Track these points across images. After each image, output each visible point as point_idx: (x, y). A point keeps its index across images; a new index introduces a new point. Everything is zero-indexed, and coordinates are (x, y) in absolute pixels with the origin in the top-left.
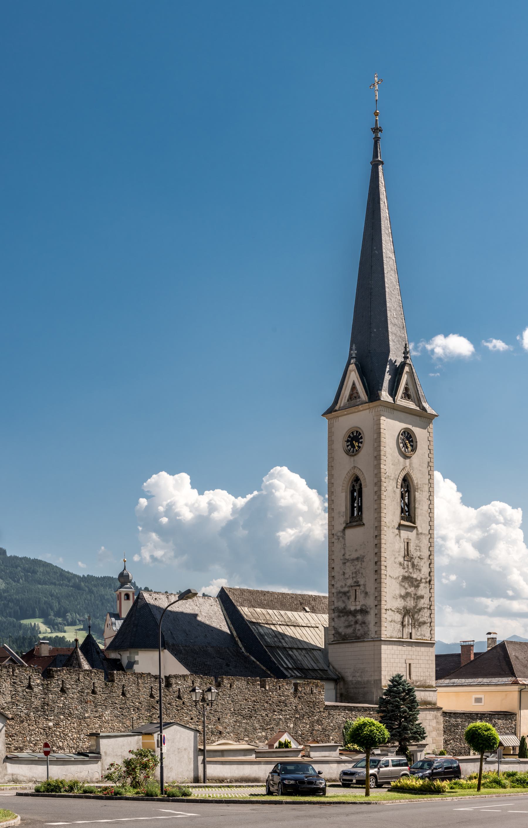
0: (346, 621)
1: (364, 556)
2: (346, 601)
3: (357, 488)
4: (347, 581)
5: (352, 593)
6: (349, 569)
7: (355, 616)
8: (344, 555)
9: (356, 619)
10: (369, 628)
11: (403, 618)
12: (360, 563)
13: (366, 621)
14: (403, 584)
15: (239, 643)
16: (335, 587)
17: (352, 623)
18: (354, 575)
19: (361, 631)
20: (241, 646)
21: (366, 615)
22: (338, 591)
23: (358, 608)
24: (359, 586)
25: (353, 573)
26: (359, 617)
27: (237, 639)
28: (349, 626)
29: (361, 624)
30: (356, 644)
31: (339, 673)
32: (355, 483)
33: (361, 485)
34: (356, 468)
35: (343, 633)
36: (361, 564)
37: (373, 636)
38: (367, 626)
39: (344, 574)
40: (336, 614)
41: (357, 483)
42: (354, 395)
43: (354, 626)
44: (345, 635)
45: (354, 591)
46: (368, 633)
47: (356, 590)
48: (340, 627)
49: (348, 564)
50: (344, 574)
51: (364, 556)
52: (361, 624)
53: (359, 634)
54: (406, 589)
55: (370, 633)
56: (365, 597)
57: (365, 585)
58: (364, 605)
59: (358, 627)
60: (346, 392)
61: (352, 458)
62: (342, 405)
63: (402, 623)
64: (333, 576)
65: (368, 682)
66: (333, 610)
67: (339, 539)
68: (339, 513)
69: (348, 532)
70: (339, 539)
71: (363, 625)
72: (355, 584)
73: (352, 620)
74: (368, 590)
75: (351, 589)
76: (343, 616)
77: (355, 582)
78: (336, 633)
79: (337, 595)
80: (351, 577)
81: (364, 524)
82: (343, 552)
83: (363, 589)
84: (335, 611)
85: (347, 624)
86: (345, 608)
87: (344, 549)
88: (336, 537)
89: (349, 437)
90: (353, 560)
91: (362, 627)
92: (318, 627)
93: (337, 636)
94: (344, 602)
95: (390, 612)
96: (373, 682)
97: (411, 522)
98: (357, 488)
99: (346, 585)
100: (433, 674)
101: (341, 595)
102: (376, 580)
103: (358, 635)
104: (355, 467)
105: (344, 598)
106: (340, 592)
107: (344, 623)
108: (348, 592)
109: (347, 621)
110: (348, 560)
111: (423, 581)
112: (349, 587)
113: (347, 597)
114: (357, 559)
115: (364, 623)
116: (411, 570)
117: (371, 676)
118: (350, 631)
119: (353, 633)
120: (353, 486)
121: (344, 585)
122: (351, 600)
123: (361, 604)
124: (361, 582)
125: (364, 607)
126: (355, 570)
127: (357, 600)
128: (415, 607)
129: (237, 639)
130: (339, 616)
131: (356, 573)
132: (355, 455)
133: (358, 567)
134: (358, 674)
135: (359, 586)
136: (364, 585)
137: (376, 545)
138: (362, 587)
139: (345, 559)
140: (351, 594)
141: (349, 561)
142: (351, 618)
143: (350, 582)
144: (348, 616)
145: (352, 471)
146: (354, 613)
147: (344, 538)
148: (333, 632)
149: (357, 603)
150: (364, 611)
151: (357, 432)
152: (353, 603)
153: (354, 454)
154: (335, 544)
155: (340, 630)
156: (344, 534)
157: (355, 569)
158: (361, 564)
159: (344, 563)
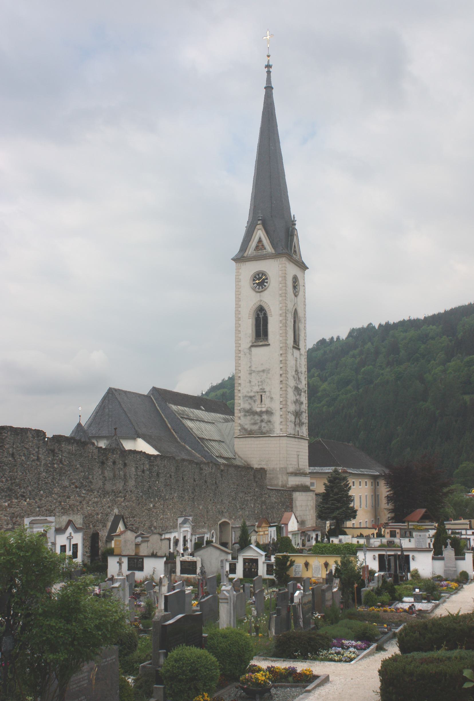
0: (252, 419)
1: (269, 370)
2: (253, 403)
4: (254, 387)
5: (258, 398)
7: (261, 416)
8: (250, 367)
9: (262, 418)
10: (274, 426)
11: (295, 419)
12: (265, 374)
13: (272, 420)
14: (295, 392)
15: (174, 433)
16: (241, 392)
17: (259, 421)
18: (260, 384)
19: (267, 428)
20: (176, 436)
21: (271, 415)
22: (245, 395)
23: (264, 409)
24: (265, 392)
25: (258, 382)
26: (265, 417)
27: (172, 431)
28: (255, 424)
29: (266, 423)
30: (262, 438)
31: (245, 461)
32: (258, 312)
33: (265, 314)
34: (262, 302)
35: (249, 429)
36: (267, 375)
37: (278, 432)
38: (272, 424)
39: (250, 382)
41: (261, 313)
42: (260, 245)
43: (259, 424)
44: (251, 431)
45: (260, 396)
46: (274, 430)
47: (261, 396)
48: (246, 424)
49: (253, 374)
50: (250, 382)
51: (269, 370)
52: (266, 423)
53: (264, 430)
54: (296, 396)
55: (275, 430)
56: (271, 401)
57: (270, 392)
58: (270, 407)
59: (263, 424)
61: (258, 294)
62: (250, 253)
63: (295, 422)
64: (240, 384)
65: (274, 469)
66: (240, 410)
67: (245, 354)
69: (253, 349)
70: (245, 354)
71: (269, 423)
72: (261, 391)
73: (258, 419)
74: (273, 396)
75: (256, 394)
76: (249, 415)
77: (261, 389)
78: (242, 429)
79: (244, 399)
80: (257, 385)
81: (269, 345)
82: (249, 365)
83: (269, 395)
84: (241, 411)
85: (253, 422)
86: (251, 409)
87: (251, 362)
88: (242, 353)
91: (268, 425)
92: (214, 423)
93: (243, 431)
94: (250, 404)
95: (289, 414)
96: (278, 470)
97: (296, 345)
99: (251, 391)
100: (307, 464)
101: (247, 398)
102: (281, 388)
103: (264, 431)
104: (261, 301)
105: (250, 401)
106: (246, 396)
107: (250, 421)
108: (254, 396)
109: (254, 419)
110: (254, 371)
111: (303, 390)
113: (253, 401)
114: (263, 371)
115: (270, 421)
116: (298, 382)
117: (277, 464)
118: (255, 428)
119: (259, 429)
120: (258, 315)
121: (250, 391)
122: (257, 403)
123: (266, 407)
124: (267, 389)
125: (269, 409)
126: (261, 380)
127: (263, 403)
128: (300, 410)
129: (172, 431)
130: (245, 415)
131: (262, 382)
132: (262, 292)
134: (264, 463)
135: (265, 392)
136: (269, 391)
137: (281, 361)
138: (267, 393)
139: (252, 370)
140: (257, 398)
141: (255, 372)
142: (257, 417)
143: (256, 389)
144: (254, 415)
145: (259, 303)
146: (260, 414)
147: (250, 354)
148: (239, 428)
149: (263, 406)
150: (269, 412)
152: (260, 406)
153: (260, 290)
154: (241, 359)
155: (246, 427)
156: (251, 351)
157: (261, 378)
158: (267, 375)
159: (250, 374)
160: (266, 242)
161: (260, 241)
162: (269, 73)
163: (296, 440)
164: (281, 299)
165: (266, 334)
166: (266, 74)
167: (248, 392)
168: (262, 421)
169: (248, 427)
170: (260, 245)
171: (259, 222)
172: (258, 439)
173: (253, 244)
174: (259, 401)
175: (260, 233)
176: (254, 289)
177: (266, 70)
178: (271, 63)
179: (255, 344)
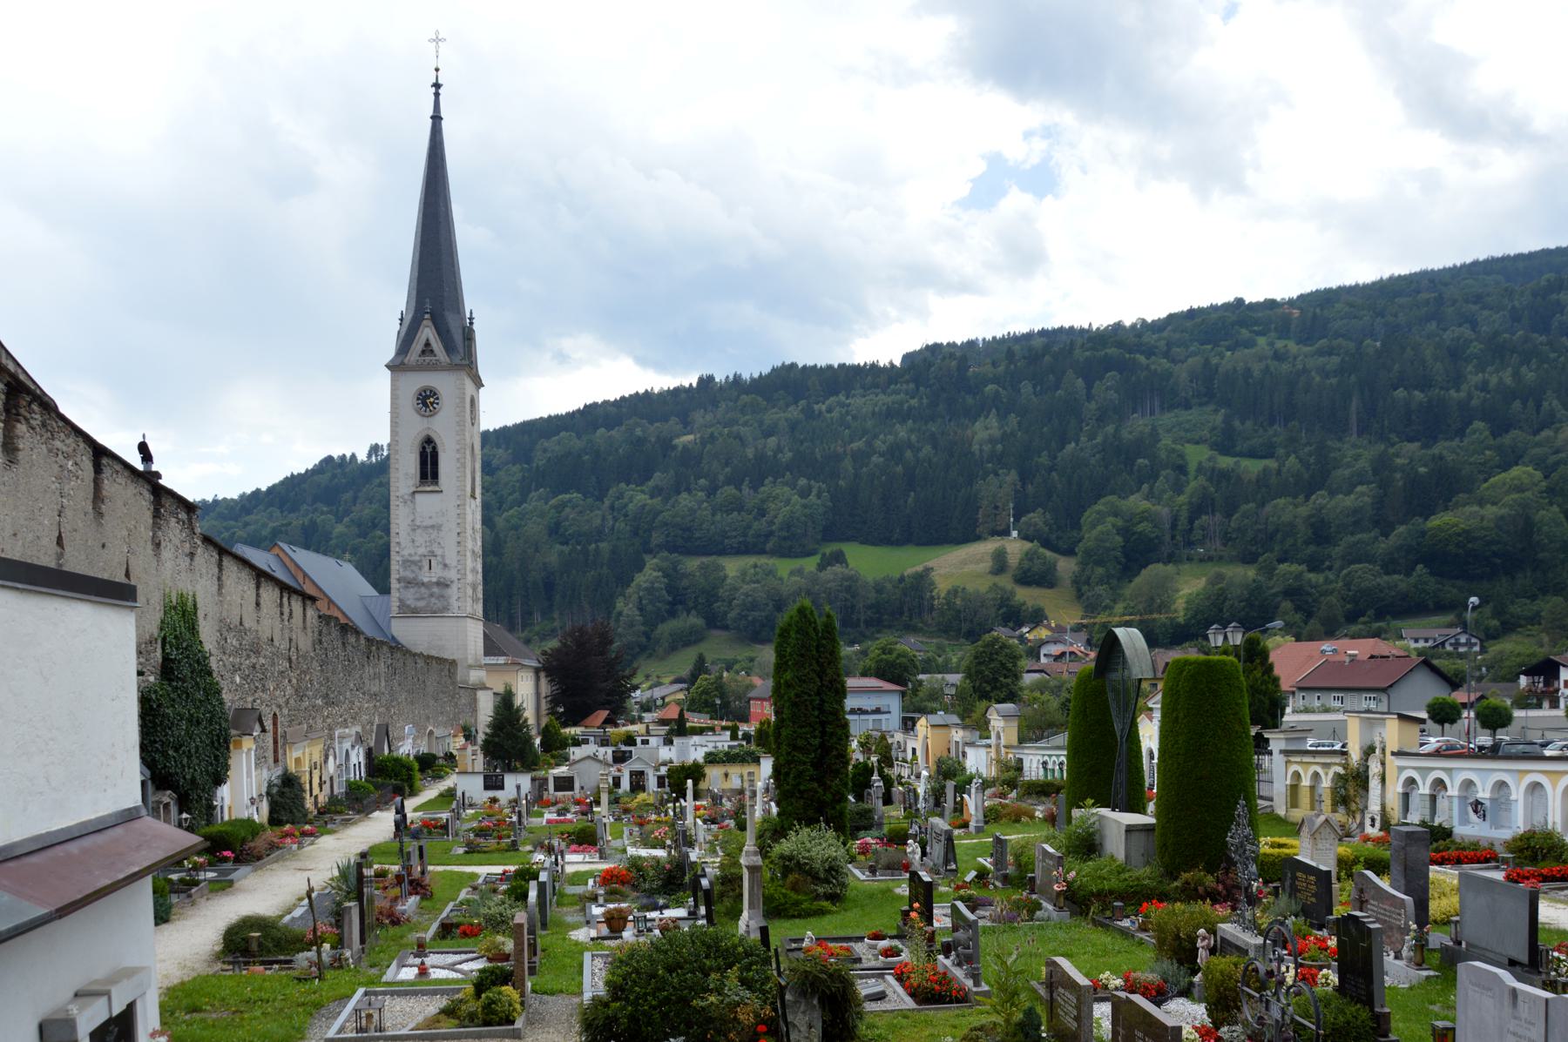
1: (441, 525)
3: (429, 450)
6: (421, 538)
19: (439, 605)
23: (434, 580)
24: (436, 556)
26: (435, 590)
33: (434, 448)
40: (402, 584)
42: (427, 349)
44: (415, 608)
49: (419, 531)
50: (413, 541)
51: (441, 525)
57: (443, 557)
60: (418, 346)
61: (425, 419)
68: (407, 474)
74: (447, 562)
82: (412, 517)
89: (420, 394)
90: (426, 527)
98: (429, 450)
108: (420, 561)
110: (419, 527)
112: (420, 556)
114: (433, 527)
115: (442, 596)
118: (421, 604)
120: (424, 448)
124: (439, 552)
131: (430, 541)
133: (433, 536)
135: (436, 556)
142: (423, 590)
143: (422, 551)
149: (433, 575)
150: (443, 584)
151: (431, 391)
152: (427, 574)
153: (427, 414)
159: (414, 530)
160: (437, 345)
161: (427, 344)
162: (437, 95)
163: (475, 621)
164: (458, 428)
165: (435, 476)
166: (433, 97)
167: (410, 555)
168: (432, 595)
169: (411, 602)
170: (427, 349)
171: (427, 316)
172: (426, 620)
173: (418, 346)
174: (427, 567)
175: (428, 332)
176: (418, 412)
177: (434, 89)
178: (440, 82)
179: (419, 489)
